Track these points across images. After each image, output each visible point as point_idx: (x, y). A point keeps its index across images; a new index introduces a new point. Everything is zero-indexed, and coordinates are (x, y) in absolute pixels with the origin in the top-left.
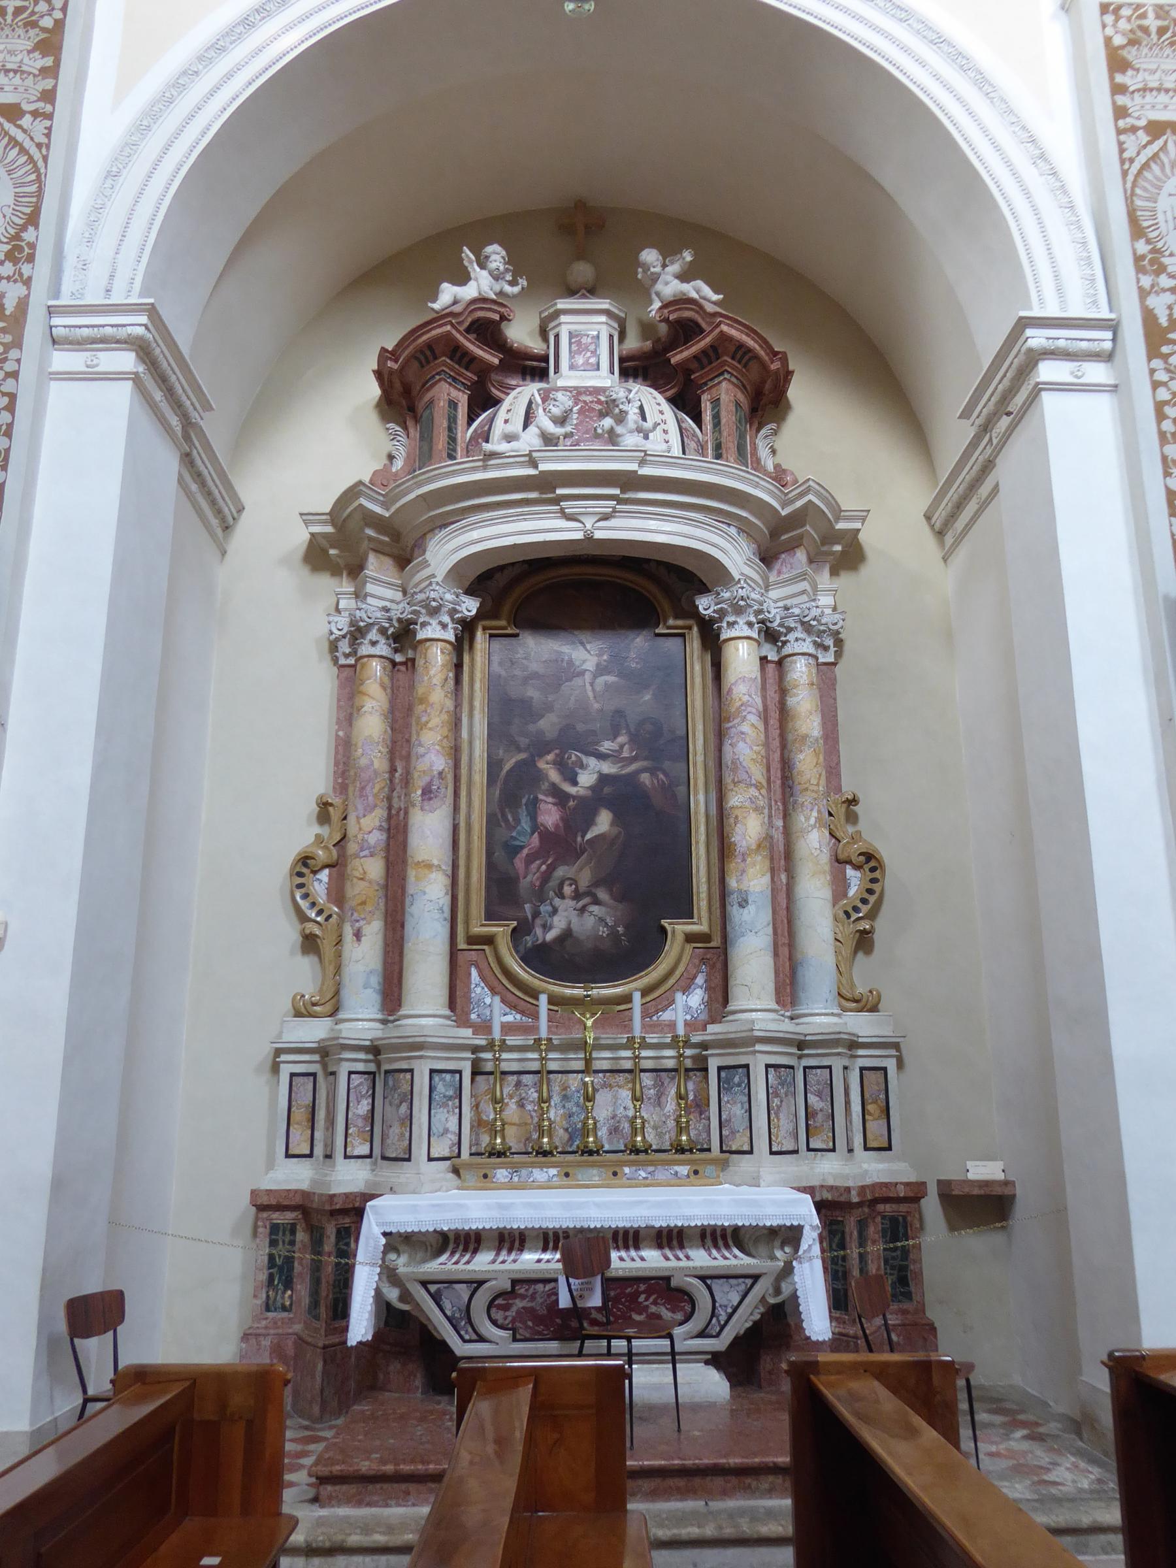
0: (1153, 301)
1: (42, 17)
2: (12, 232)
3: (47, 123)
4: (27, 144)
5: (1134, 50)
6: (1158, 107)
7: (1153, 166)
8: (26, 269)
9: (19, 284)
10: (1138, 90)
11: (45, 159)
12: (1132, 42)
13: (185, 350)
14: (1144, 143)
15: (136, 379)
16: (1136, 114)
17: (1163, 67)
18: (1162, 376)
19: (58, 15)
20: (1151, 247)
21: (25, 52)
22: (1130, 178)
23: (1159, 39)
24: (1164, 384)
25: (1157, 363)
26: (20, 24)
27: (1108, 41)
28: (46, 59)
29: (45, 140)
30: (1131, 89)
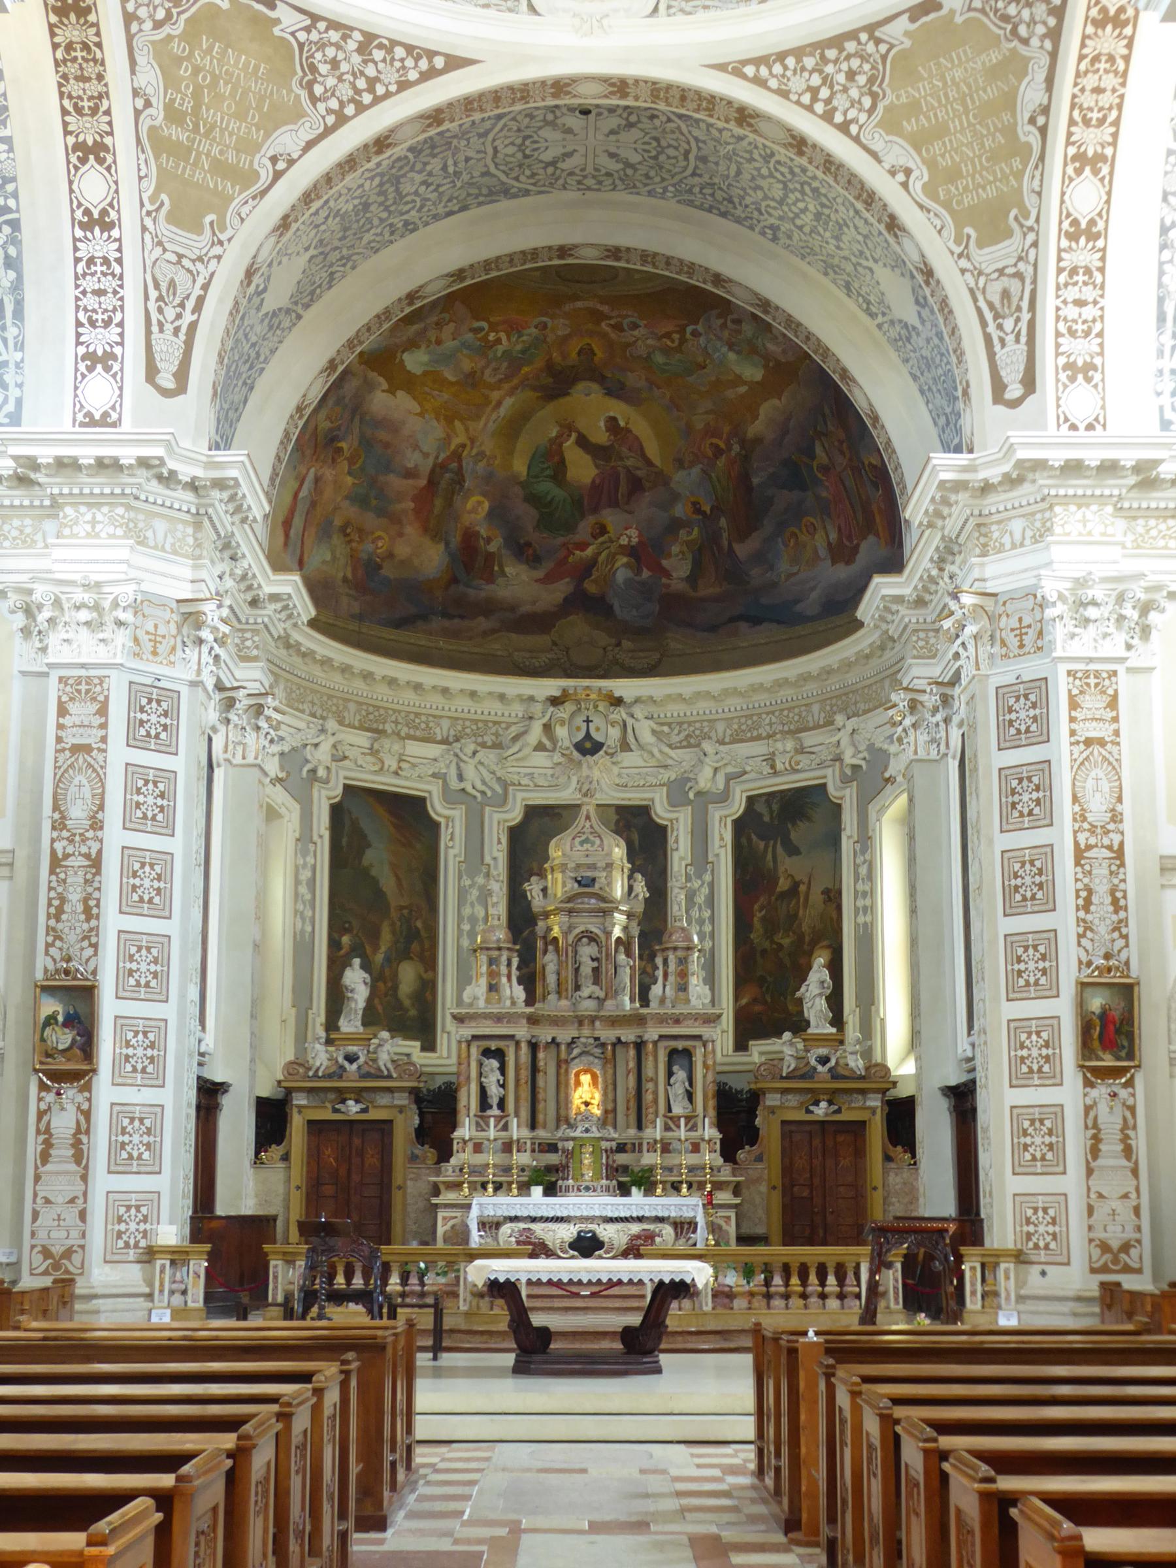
12: (1081, 692)
25: (1079, 869)
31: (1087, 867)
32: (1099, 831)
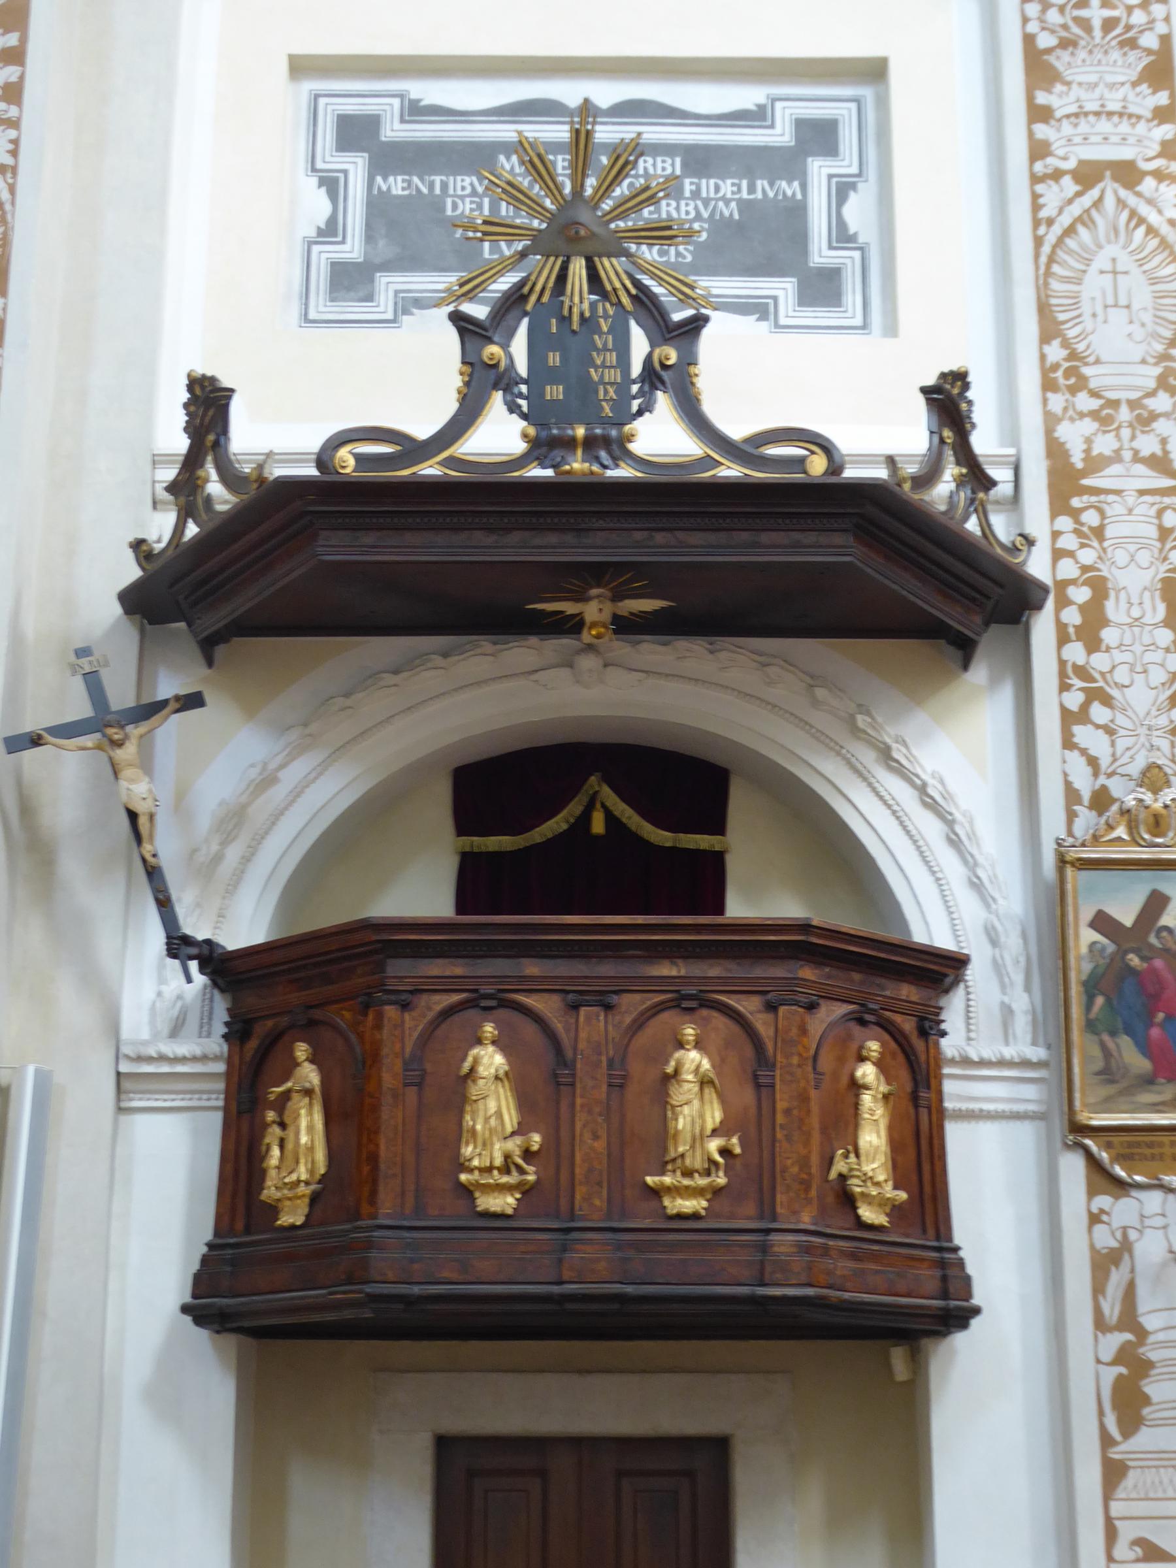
5: (1065, 55)
6: (1093, 139)
7: (1081, 229)
10: (1068, 116)
14: (1070, 194)
16: (1061, 152)
18: (1068, 542)
20: (1065, 353)
22: (1046, 249)
23: (1103, 38)
24: (1070, 554)
25: (1064, 523)
27: (1029, 40)
31: (1091, 518)
32: (1124, 414)
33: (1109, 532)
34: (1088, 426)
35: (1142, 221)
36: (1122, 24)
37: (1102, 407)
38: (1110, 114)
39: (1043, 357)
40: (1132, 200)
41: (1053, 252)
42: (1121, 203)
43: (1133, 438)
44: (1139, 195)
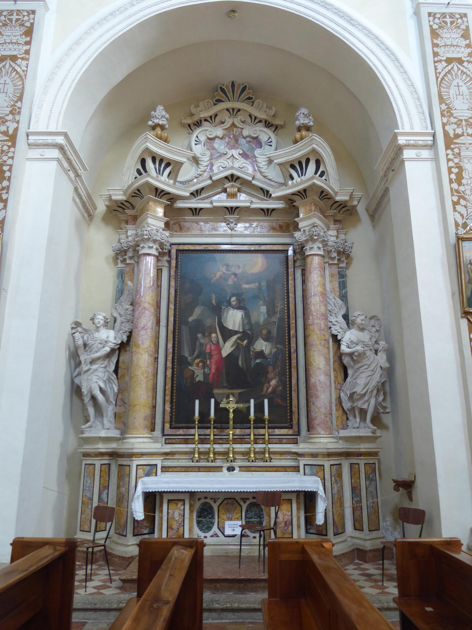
0: (447, 128)
1: (26, 22)
2: (12, 103)
3: (27, 62)
4: (19, 69)
8: (17, 117)
9: (15, 123)
10: (443, 46)
11: (26, 75)
12: (440, 27)
13: (77, 148)
14: (445, 66)
15: (58, 160)
17: (452, 36)
18: (451, 157)
19: (32, 21)
20: (447, 107)
21: (19, 36)
22: (439, 79)
23: (451, 26)
24: (452, 160)
25: (449, 152)
26: (18, 25)
27: (431, 26)
28: (27, 38)
29: (25, 69)
30: (440, 45)
31: (457, 151)
32: (464, 123)
33: (462, 154)
34: (454, 126)
35: (464, 73)
36: (455, 23)
37: (458, 121)
38: (454, 46)
39: (440, 108)
40: (462, 68)
41: (441, 81)
42: (459, 69)
43: (467, 129)
44: (463, 66)
